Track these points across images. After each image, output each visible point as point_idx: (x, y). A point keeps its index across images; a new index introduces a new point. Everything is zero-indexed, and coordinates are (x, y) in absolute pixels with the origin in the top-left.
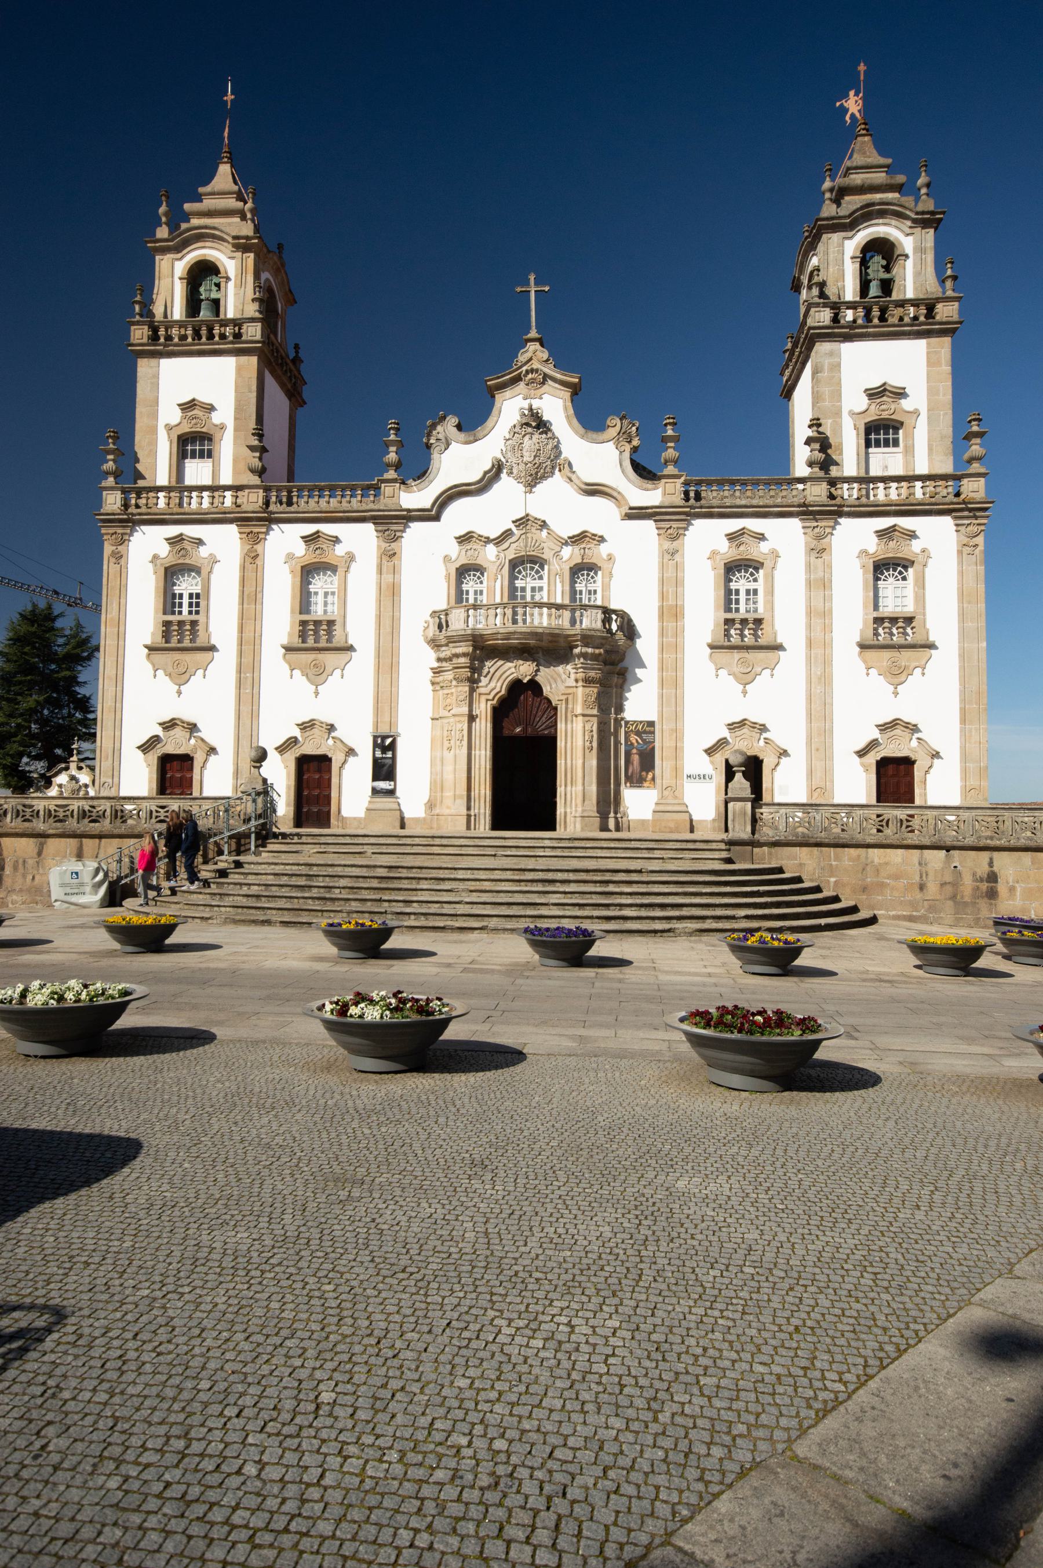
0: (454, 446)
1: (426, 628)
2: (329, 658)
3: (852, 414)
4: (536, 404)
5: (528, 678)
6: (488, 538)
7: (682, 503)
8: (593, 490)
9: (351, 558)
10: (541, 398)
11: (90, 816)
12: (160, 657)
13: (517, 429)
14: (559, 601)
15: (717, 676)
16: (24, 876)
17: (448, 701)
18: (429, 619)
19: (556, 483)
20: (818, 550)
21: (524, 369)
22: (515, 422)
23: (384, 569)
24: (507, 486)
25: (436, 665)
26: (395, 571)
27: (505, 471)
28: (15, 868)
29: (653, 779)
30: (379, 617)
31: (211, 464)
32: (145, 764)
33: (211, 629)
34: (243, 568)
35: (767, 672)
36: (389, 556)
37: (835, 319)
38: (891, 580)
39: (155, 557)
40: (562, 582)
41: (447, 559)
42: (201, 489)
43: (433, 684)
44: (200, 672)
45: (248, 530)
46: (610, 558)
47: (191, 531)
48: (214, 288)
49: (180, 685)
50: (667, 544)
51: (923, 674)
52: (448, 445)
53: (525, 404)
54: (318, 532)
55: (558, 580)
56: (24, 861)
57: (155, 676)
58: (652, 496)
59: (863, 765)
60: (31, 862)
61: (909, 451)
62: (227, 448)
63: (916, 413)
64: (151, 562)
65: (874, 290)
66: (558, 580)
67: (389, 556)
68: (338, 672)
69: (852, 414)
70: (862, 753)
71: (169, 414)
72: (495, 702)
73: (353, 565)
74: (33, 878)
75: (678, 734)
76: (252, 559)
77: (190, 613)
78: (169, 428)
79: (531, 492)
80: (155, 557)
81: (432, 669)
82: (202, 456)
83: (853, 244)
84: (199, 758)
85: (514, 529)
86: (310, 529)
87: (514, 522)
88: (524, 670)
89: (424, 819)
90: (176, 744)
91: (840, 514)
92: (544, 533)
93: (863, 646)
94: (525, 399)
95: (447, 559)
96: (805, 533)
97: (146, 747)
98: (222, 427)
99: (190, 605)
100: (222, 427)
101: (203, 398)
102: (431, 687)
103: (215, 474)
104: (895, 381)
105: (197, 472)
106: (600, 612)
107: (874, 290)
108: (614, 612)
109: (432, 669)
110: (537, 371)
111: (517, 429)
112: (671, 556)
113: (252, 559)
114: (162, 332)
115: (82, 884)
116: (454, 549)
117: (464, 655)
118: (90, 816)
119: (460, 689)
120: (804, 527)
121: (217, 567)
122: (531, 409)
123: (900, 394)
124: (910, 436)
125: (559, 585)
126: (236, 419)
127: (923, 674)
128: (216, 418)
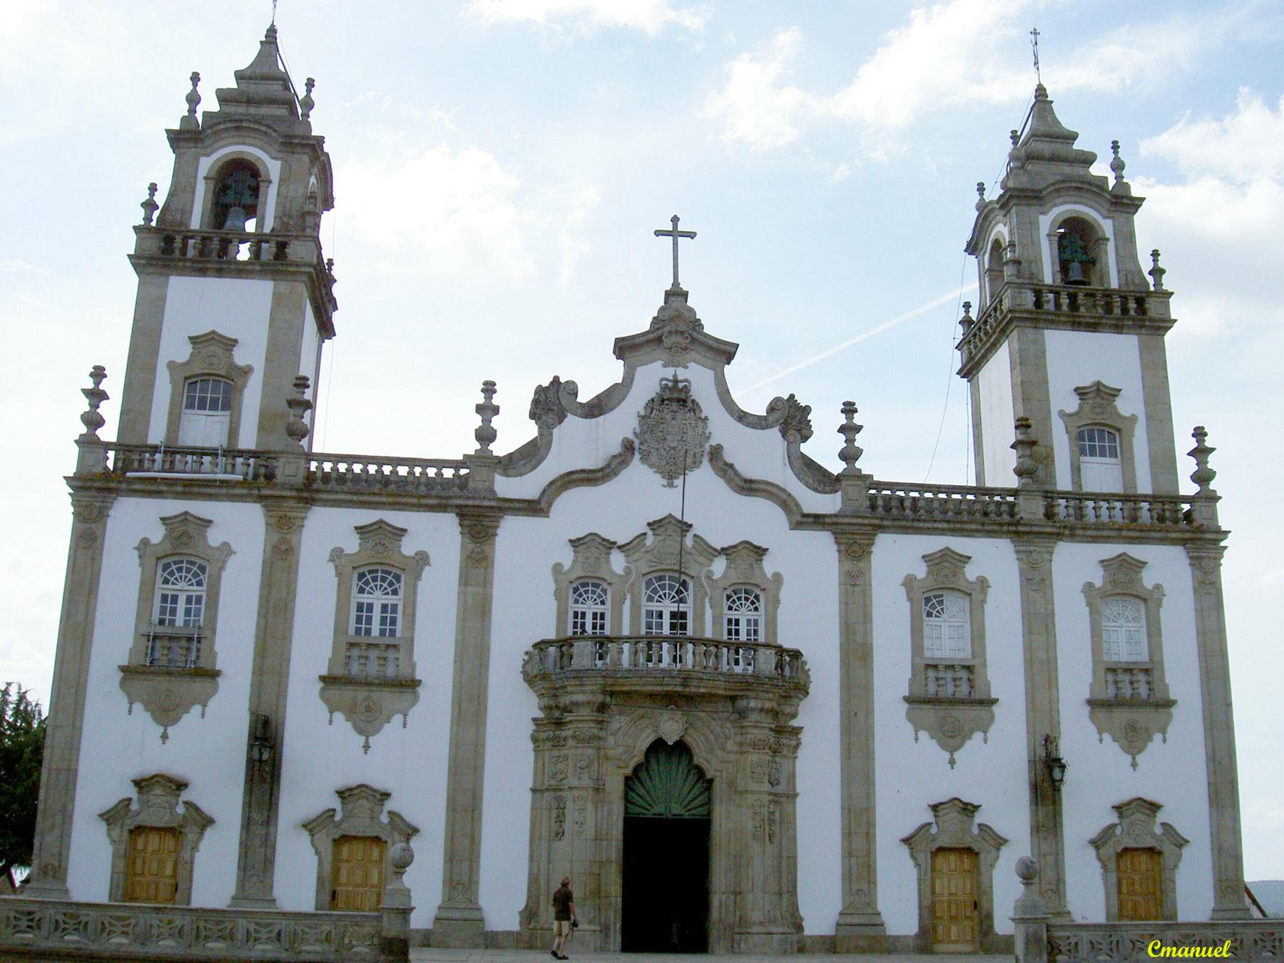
1: (526, 663)
2: (386, 698)
3: (1062, 414)
4: (682, 374)
5: (676, 738)
6: (615, 543)
7: (868, 513)
8: (748, 487)
9: (422, 559)
10: (686, 367)
11: (32, 920)
12: (140, 685)
14: (708, 634)
15: (916, 739)
17: (560, 766)
18: (531, 649)
19: (703, 478)
21: (667, 329)
22: (653, 395)
24: (639, 474)
26: (487, 583)
27: (637, 456)
31: (227, 420)
32: (107, 840)
35: (978, 736)
37: (1038, 304)
38: (1122, 621)
39: (145, 543)
41: (557, 568)
44: (196, 709)
46: (778, 578)
49: (166, 727)
50: (848, 565)
51: (1164, 740)
52: (561, 419)
53: (669, 373)
55: (707, 605)
57: (130, 712)
59: (1099, 858)
62: (252, 398)
63: (1133, 419)
64: (137, 548)
65: (1075, 274)
66: (707, 605)
68: (398, 719)
69: (1062, 414)
70: (1097, 843)
73: (427, 569)
78: (172, 366)
79: (671, 485)
80: (145, 543)
81: (534, 720)
83: (1047, 221)
85: (650, 533)
86: (367, 516)
87: (649, 524)
88: (670, 727)
89: (519, 933)
91: (1059, 536)
92: (689, 541)
93: (1093, 703)
94: (665, 366)
95: (557, 568)
96: (1018, 559)
97: (110, 817)
98: (246, 371)
99: (188, 612)
100: (246, 371)
102: (531, 746)
103: (233, 432)
104: (1110, 382)
106: (773, 652)
107: (1075, 274)
108: (787, 651)
109: (534, 720)
110: (682, 333)
114: (178, 244)
116: (567, 558)
117: (589, 703)
118: (32, 920)
119: (580, 751)
120: (1017, 552)
121: (232, 563)
122: (676, 381)
123: (1115, 393)
126: (267, 360)
127: (1164, 740)
128: (241, 357)
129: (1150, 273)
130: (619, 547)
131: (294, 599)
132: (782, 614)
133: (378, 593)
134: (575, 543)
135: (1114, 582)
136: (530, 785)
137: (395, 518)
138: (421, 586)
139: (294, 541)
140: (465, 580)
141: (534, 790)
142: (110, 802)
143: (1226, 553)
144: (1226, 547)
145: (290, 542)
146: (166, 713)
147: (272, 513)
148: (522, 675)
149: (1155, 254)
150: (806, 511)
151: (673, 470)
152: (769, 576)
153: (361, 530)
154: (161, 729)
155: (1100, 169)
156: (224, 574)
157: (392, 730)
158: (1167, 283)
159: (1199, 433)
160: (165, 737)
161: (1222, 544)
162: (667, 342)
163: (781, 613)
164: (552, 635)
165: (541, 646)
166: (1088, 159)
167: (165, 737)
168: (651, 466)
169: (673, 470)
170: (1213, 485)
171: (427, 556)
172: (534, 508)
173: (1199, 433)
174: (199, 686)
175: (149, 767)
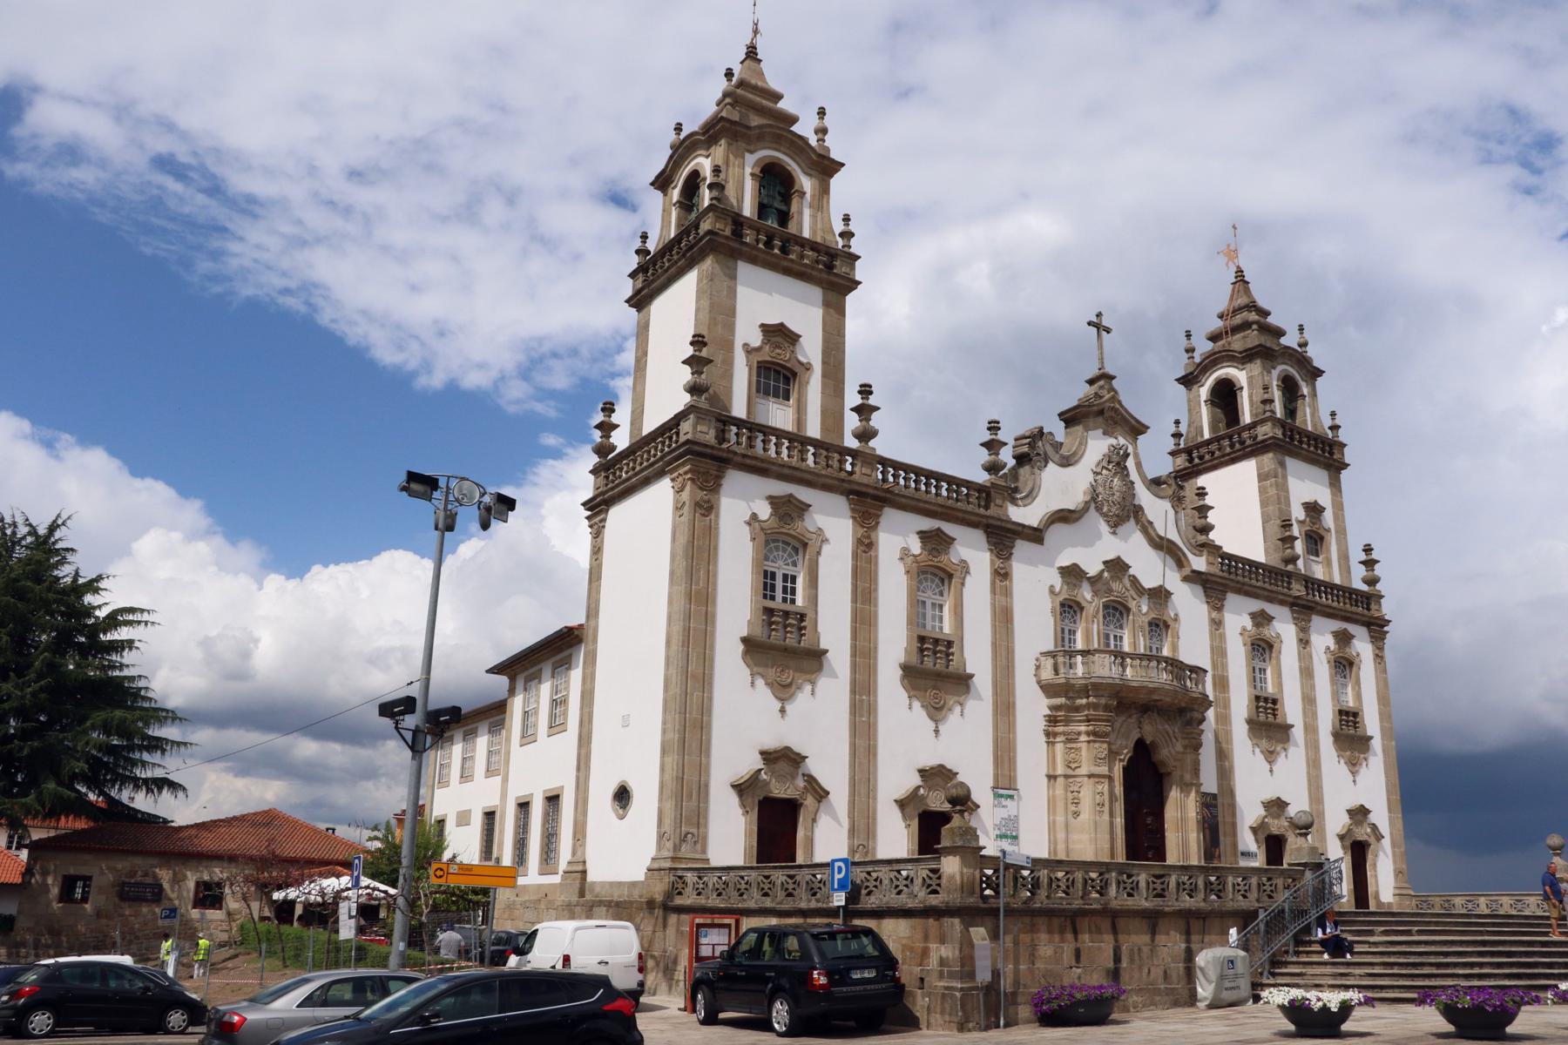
0: (1051, 465)
1: (1038, 667)
9: (965, 568)
13: (1105, 464)
16: (1140, 968)
20: (1304, 642)
23: (998, 590)
25: (1049, 712)
26: (1007, 593)
28: (1132, 961)
29: (1219, 856)
30: (994, 645)
32: (740, 811)
33: (819, 630)
34: (855, 556)
36: (1001, 575)
40: (1144, 636)
43: (1048, 734)
45: (863, 509)
46: (1176, 619)
47: (803, 494)
48: (779, 198)
50: (1214, 614)
52: (1047, 462)
54: (939, 529)
56: (1139, 950)
58: (1199, 563)
60: (1146, 950)
61: (1328, 563)
64: (749, 524)
67: (1001, 575)
71: (747, 333)
72: (1125, 763)
74: (1149, 970)
75: (1232, 806)
76: (865, 547)
77: (785, 600)
78: (749, 350)
79: (1114, 533)
82: (776, 395)
84: (809, 801)
87: (1105, 563)
97: (742, 789)
99: (785, 590)
101: (793, 326)
102: (1044, 739)
103: (800, 420)
105: (779, 416)
111: (1105, 464)
112: (1217, 624)
113: (865, 547)
115: (1236, 976)
116: (1058, 582)
119: (1097, 745)
124: (1328, 551)
125: (1142, 639)
126: (824, 363)
129: (1330, 428)
130: (1089, 578)
131: (876, 590)
132: (1182, 644)
133: (929, 593)
135: (1340, 649)
136: (1045, 771)
137: (950, 529)
138: (966, 591)
139: (874, 540)
143: (1388, 636)
144: (1387, 632)
145: (869, 537)
147: (857, 507)
148: (1034, 679)
149: (1333, 414)
150: (1195, 568)
151: (1116, 523)
152: (1172, 615)
154: (779, 705)
155: (1291, 340)
156: (821, 560)
157: (953, 719)
158: (1343, 436)
159: (1368, 549)
160: (783, 711)
161: (1386, 629)
162: (1106, 415)
163: (1181, 643)
166: (1279, 333)
167: (783, 711)
168: (1104, 515)
170: (1378, 586)
171: (968, 568)
172: (1035, 535)
173: (1368, 549)
175: (772, 743)
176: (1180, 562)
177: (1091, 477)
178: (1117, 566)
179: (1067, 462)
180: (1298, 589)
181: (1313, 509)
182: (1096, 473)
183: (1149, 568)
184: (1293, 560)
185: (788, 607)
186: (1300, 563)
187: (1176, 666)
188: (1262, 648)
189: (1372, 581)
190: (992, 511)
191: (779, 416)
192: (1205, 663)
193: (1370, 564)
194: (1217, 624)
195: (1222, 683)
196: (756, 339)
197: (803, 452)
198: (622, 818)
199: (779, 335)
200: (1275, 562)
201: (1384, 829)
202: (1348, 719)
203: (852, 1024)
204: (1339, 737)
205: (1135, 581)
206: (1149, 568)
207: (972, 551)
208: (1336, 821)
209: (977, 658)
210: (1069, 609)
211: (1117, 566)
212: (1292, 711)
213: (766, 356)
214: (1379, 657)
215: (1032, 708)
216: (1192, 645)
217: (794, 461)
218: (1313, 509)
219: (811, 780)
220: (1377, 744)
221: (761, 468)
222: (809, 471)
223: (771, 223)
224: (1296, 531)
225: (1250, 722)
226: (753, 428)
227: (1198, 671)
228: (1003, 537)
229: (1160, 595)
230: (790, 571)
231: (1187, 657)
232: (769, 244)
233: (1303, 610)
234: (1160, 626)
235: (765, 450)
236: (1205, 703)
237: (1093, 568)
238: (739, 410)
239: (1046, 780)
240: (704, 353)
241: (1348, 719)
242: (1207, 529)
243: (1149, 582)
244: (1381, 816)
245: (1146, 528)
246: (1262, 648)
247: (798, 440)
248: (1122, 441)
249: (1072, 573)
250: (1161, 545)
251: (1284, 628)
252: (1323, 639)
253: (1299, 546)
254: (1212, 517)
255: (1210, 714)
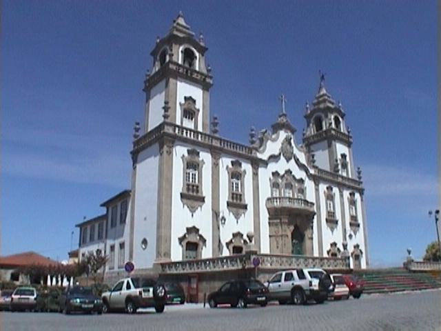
9: (245, 171)
20: (342, 196)
26: (258, 180)
36: (255, 174)
42: (191, 130)
58: (312, 171)
67: (255, 174)
76: (216, 165)
78: (180, 104)
84: (201, 243)
90: (193, 238)
97: (181, 240)
98: (198, 110)
105: (189, 124)
112: (317, 190)
113: (216, 165)
128: (197, 107)
134: (273, 174)
140: (253, 179)
141: (270, 236)
142: (181, 235)
146: (193, 210)
153: (233, 163)
164: (270, 196)
165: (268, 199)
169: (288, 160)
172: (265, 163)
174: (201, 203)
176: (307, 171)
177: (281, 145)
178: (289, 172)
179: (274, 141)
180: (340, 180)
181: (344, 156)
182: (282, 144)
183: (299, 174)
184: (338, 171)
185: (193, 183)
186: (340, 172)
187: (306, 202)
188: (330, 197)
189: (360, 178)
190: (253, 155)
191: (189, 124)
192: (314, 202)
193: (359, 173)
194: (317, 190)
195: (319, 208)
196: (183, 102)
197: (198, 136)
198: (144, 249)
199: (189, 100)
200: (332, 171)
201: (364, 251)
202: (354, 218)
203: (229, 305)
204: (351, 225)
205: (294, 177)
206: (299, 174)
207: (247, 167)
208: (351, 249)
209: (248, 199)
210: (275, 185)
211: (289, 172)
212: (338, 216)
213: (186, 106)
214: (362, 200)
215: (264, 216)
216: (311, 197)
217: (195, 139)
218: (344, 156)
219: (201, 236)
220: (361, 226)
221: (185, 141)
222: (199, 142)
223: (187, 65)
224: (339, 162)
225: (327, 220)
226: (182, 128)
227: (313, 204)
228: (257, 163)
229: (301, 181)
230: (194, 172)
231: (309, 199)
232: (187, 72)
233: (341, 186)
234: (302, 191)
235: (187, 135)
236: (315, 214)
237: (282, 173)
238: (178, 123)
239: (268, 237)
240: (216, 121)
241: (354, 218)
242: (314, 162)
243: (298, 177)
244: (362, 248)
245: (297, 161)
246: (330, 197)
247: (196, 132)
248: (290, 134)
249: (275, 174)
250: (301, 166)
251: (336, 190)
252: (346, 193)
253: (340, 167)
254: (315, 158)
255: (315, 217)
